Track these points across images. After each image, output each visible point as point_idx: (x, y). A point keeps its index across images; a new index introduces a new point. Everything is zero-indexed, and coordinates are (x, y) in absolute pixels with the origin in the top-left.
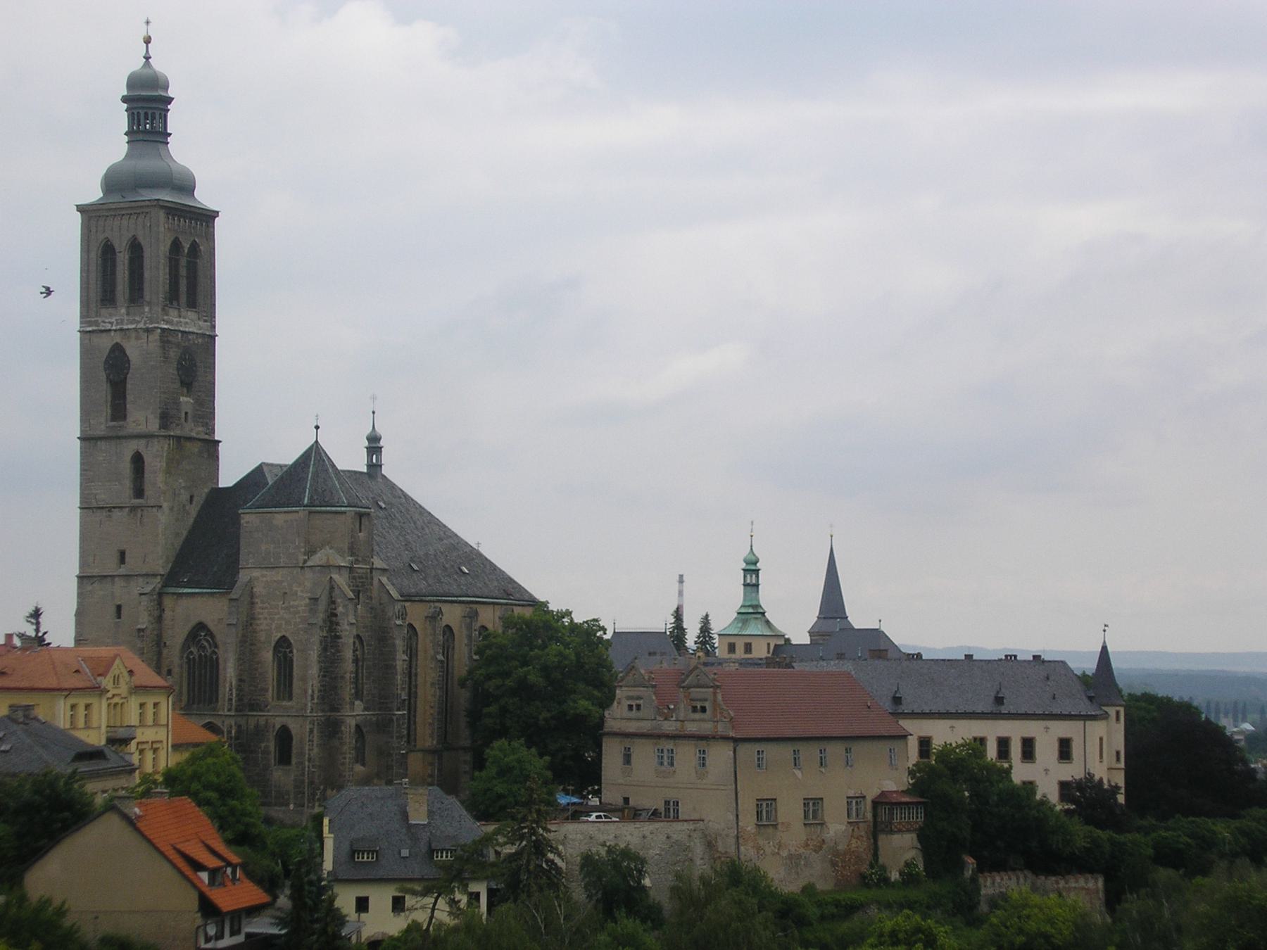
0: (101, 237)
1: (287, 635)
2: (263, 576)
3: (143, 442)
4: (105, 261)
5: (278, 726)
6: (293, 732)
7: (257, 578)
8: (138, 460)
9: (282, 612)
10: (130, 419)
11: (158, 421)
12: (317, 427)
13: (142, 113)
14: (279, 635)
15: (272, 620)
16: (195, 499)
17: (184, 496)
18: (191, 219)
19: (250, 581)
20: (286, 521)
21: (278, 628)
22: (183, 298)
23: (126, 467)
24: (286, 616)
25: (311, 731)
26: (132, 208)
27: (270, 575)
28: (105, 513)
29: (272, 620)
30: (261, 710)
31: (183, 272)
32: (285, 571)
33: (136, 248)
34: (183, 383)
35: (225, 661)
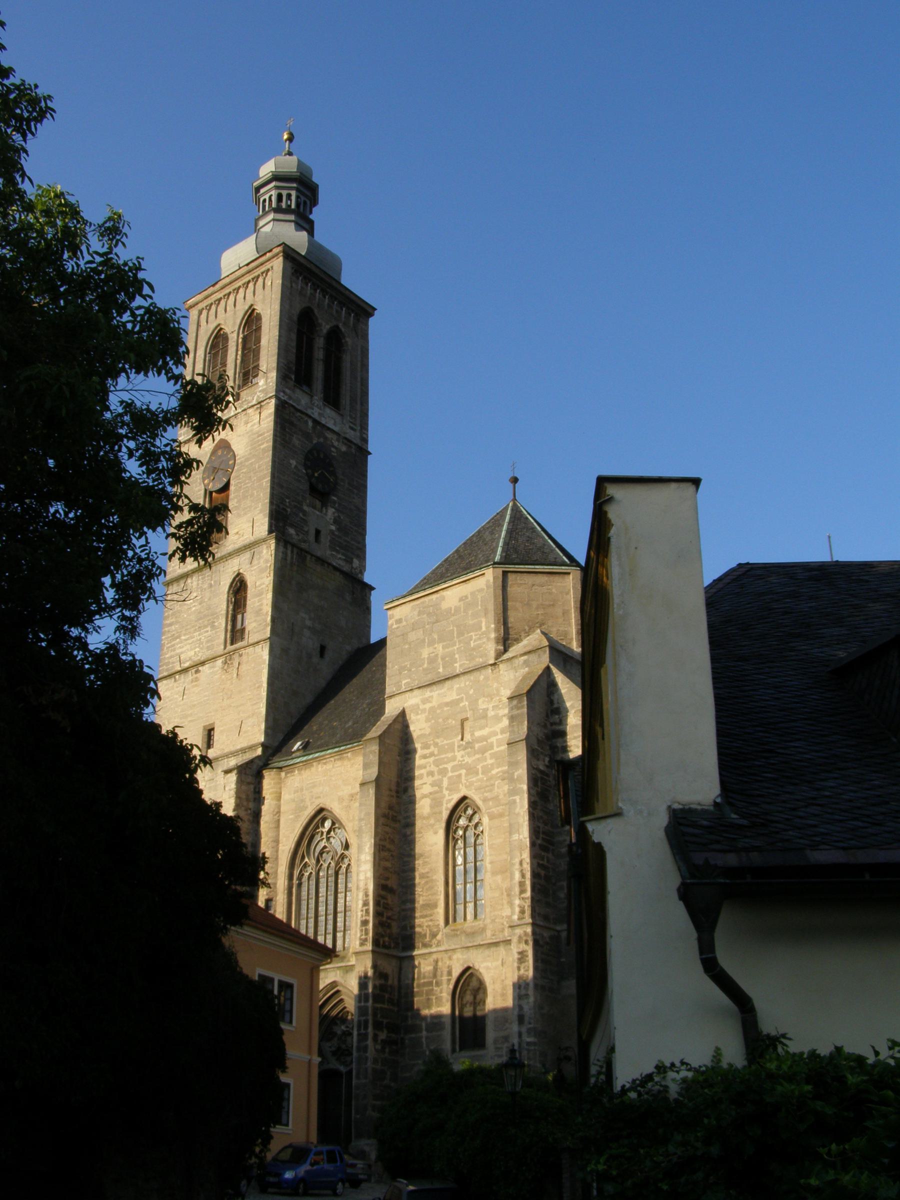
0: (212, 326)
1: (470, 793)
2: (425, 701)
3: (247, 555)
4: (215, 356)
5: (456, 974)
6: (487, 979)
7: (416, 708)
8: (239, 588)
9: (459, 755)
10: (232, 529)
11: (266, 521)
12: (515, 480)
13: (274, 193)
14: (456, 798)
15: (443, 772)
16: (329, 654)
17: (310, 642)
18: (331, 296)
19: (403, 714)
20: (461, 600)
21: (455, 783)
22: (318, 385)
23: (221, 602)
24: (468, 760)
25: (522, 955)
26: (249, 272)
27: (437, 695)
28: (190, 676)
29: (443, 772)
30: (425, 945)
31: (319, 354)
32: (463, 682)
33: (252, 320)
34: (313, 490)
35: (360, 849)
